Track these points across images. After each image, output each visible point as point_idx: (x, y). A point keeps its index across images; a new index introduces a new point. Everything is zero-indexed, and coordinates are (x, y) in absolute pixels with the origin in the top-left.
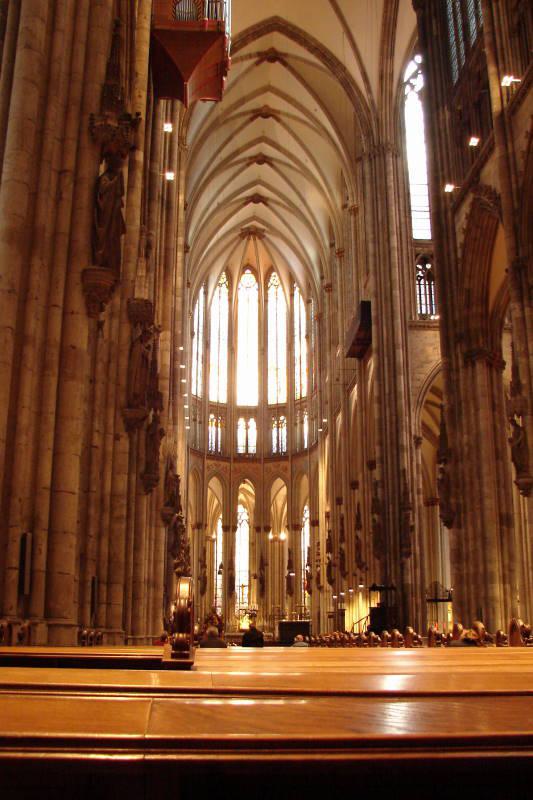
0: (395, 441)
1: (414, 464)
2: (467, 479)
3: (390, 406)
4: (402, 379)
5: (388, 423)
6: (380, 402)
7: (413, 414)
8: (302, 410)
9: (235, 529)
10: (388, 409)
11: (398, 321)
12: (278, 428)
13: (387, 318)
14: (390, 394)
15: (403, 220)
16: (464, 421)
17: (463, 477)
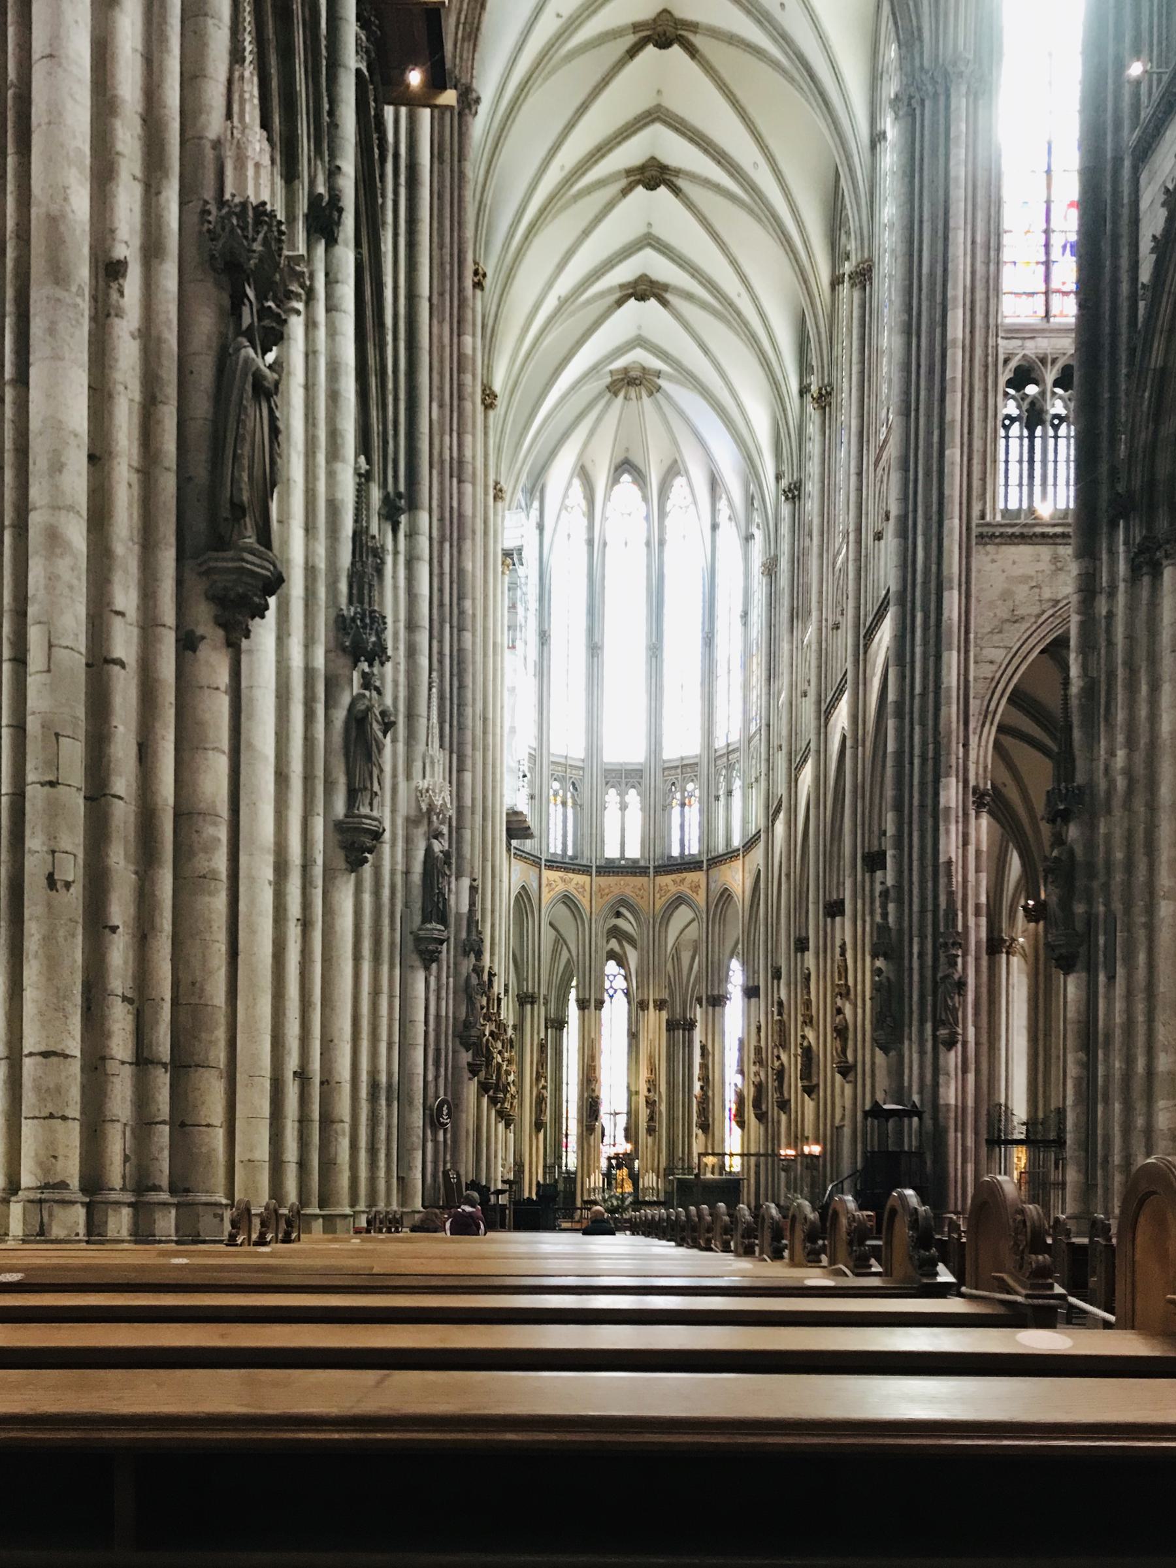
0: (929, 802)
1: (972, 849)
2: (1119, 855)
3: (923, 725)
4: (952, 659)
5: (916, 761)
6: (899, 715)
7: (973, 740)
8: (730, 767)
9: (600, 1004)
10: (917, 728)
11: (954, 525)
12: (683, 805)
13: (928, 519)
14: (924, 694)
15: (980, 267)
16: (1120, 716)
17: (1109, 852)
